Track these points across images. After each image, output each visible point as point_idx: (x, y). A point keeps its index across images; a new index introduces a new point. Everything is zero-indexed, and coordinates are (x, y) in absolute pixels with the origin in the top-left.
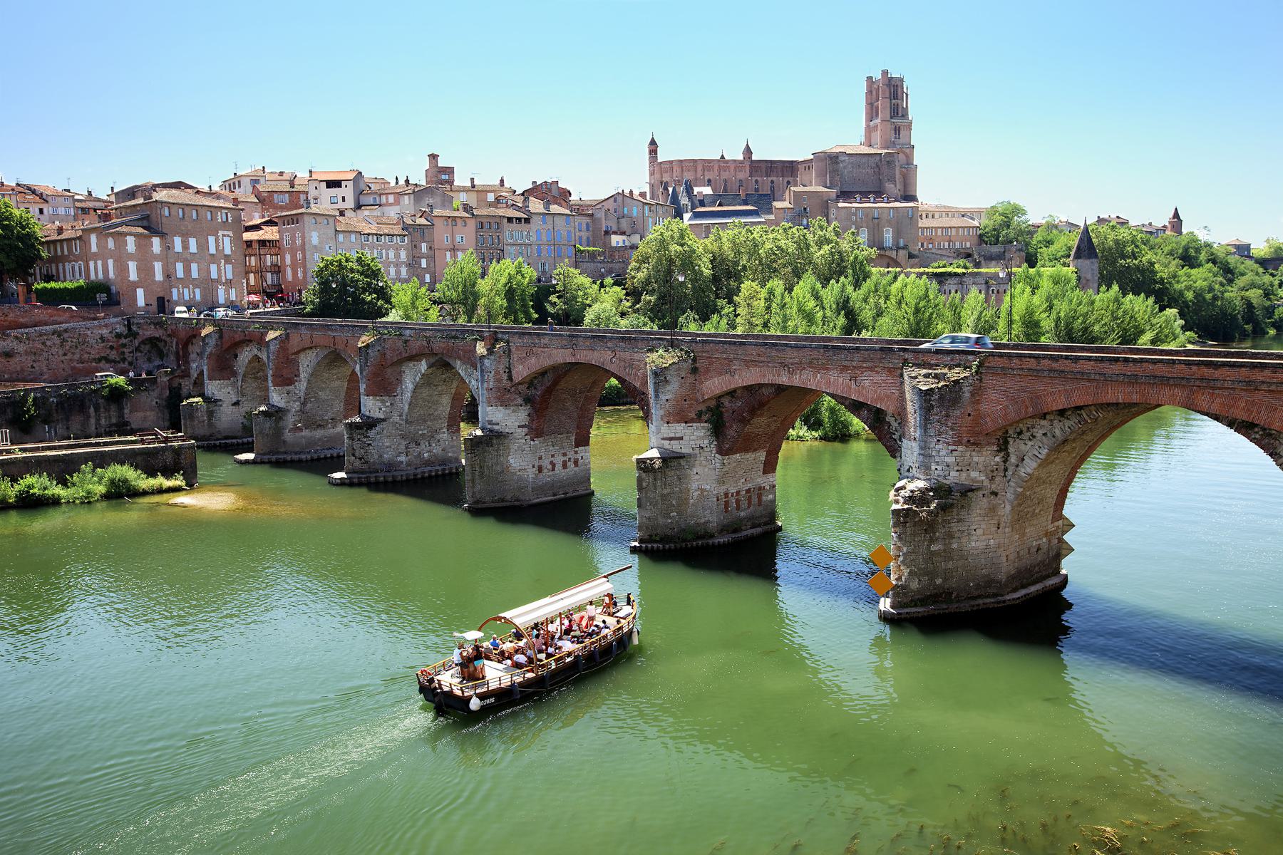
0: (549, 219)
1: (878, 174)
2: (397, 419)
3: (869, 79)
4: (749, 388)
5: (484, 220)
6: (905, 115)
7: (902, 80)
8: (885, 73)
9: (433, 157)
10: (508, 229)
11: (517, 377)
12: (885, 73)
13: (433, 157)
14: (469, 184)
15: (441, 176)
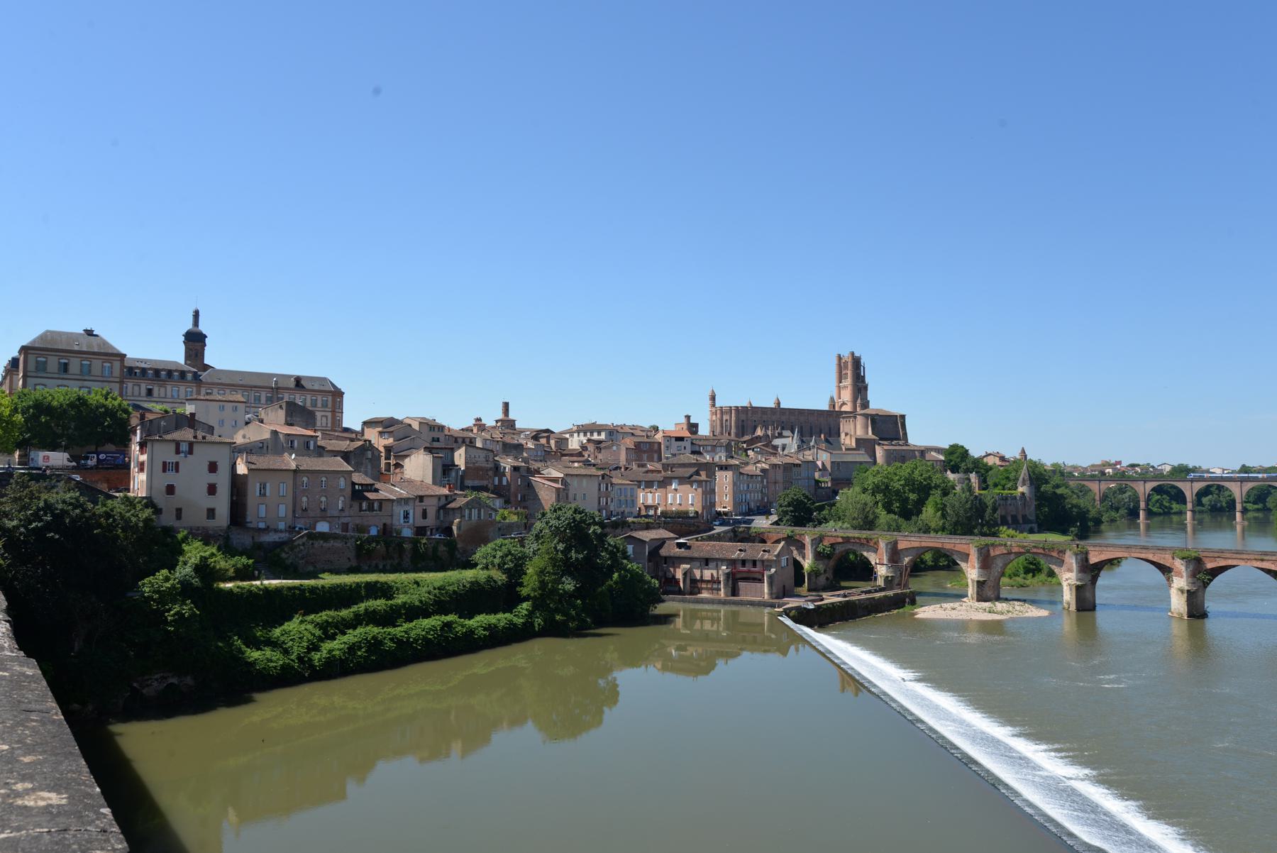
3: (840, 358)
6: (864, 381)
9: (688, 417)
10: (794, 469)
12: (853, 354)
13: (688, 417)
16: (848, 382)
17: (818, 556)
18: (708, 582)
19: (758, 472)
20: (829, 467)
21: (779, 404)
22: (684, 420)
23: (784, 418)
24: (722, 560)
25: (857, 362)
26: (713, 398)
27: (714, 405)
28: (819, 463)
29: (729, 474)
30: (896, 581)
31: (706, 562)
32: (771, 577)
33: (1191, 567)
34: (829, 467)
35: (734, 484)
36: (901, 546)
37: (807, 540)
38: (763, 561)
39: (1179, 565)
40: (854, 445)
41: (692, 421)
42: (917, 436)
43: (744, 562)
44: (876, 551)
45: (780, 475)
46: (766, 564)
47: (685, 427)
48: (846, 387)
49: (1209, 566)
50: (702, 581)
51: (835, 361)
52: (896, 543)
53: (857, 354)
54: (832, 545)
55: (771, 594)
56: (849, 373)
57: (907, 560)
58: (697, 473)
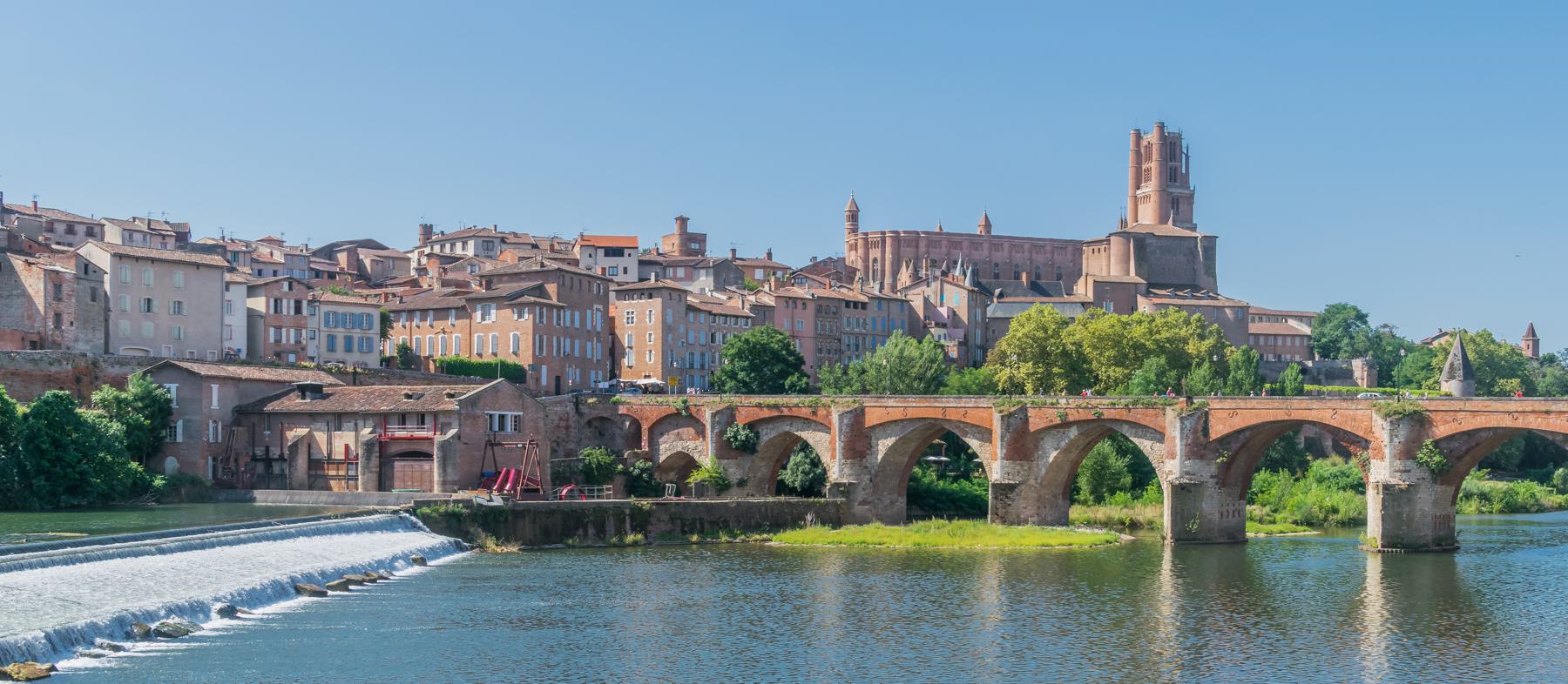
0: (884, 304)
1: (1173, 264)
2: (1032, 482)
3: (1138, 136)
4: (1469, 434)
5: (824, 303)
7: (1179, 137)
8: (1162, 127)
9: (683, 221)
11: (1214, 435)
12: (1162, 127)
13: (683, 221)
14: (730, 256)
15: (693, 243)
16: (1150, 187)
17: (726, 449)
18: (339, 463)
19: (747, 311)
20: (965, 318)
21: (988, 225)
22: (675, 229)
23: (1001, 256)
24: (366, 416)
25: (1172, 148)
26: (854, 217)
27: (854, 230)
28: (944, 311)
29: (657, 302)
30: (860, 495)
31: (338, 419)
32: (444, 446)
33: (1403, 432)
34: (965, 318)
35: (667, 329)
36: (872, 418)
37: (707, 417)
38: (435, 415)
39: (1380, 431)
40: (1090, 297)
41: (692, 228)
42: (1235, 284)
43: (403, 418)
44: (826, 428)
45: (806, 322)
46: (438, 419)
47: (677, 241)
48: (1147, 197)
49: (1442, 430)
50: (330, 460)
51: (1132, 146)
52: (859, 414)
53: (1171, 128)
54: (751, 426)
55: (444, 483)
56: (1153, 165)
57: (884, 445)
58: (540, 291)
